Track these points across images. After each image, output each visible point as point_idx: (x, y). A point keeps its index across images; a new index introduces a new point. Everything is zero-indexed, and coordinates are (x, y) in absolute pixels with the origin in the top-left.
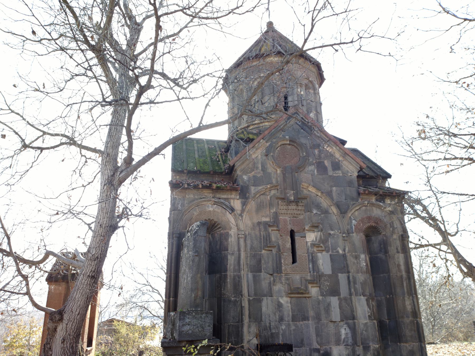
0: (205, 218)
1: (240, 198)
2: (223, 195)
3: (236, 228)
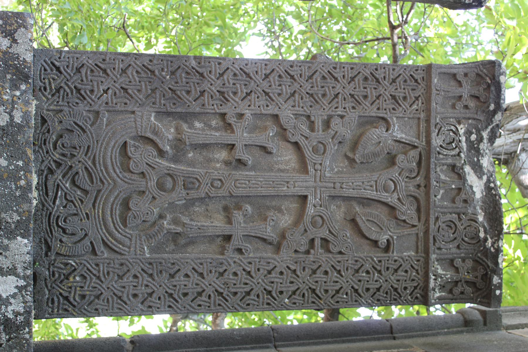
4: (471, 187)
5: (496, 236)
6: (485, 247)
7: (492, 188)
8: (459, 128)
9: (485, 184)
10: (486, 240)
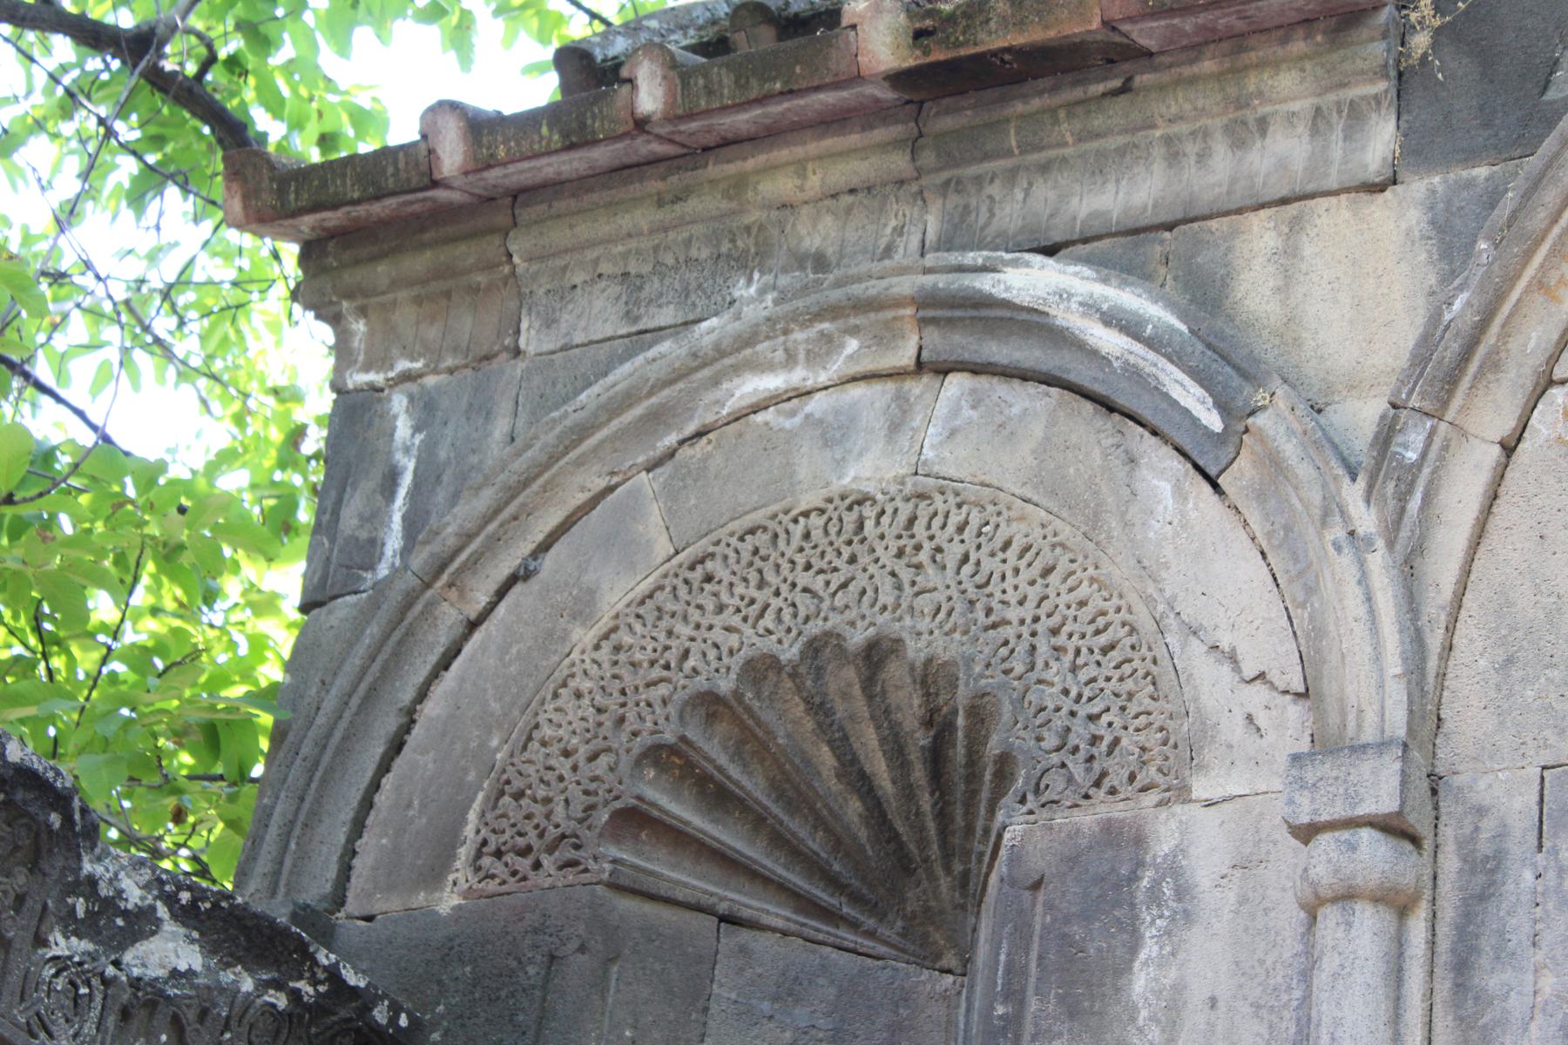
0: (752, 642)
1: (1418, 150)
2: (1098, 168)
3: (1290, 726)
4: (175, 973)
5: (303, 963)
6: (308, 1007)
7: (194, 902)
8: (56, 951)
9: (174, 916)
10: (295, 995)
